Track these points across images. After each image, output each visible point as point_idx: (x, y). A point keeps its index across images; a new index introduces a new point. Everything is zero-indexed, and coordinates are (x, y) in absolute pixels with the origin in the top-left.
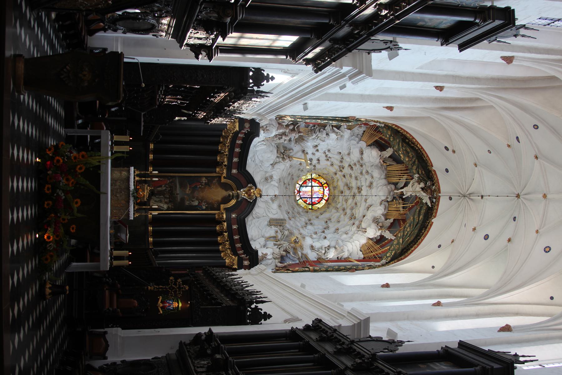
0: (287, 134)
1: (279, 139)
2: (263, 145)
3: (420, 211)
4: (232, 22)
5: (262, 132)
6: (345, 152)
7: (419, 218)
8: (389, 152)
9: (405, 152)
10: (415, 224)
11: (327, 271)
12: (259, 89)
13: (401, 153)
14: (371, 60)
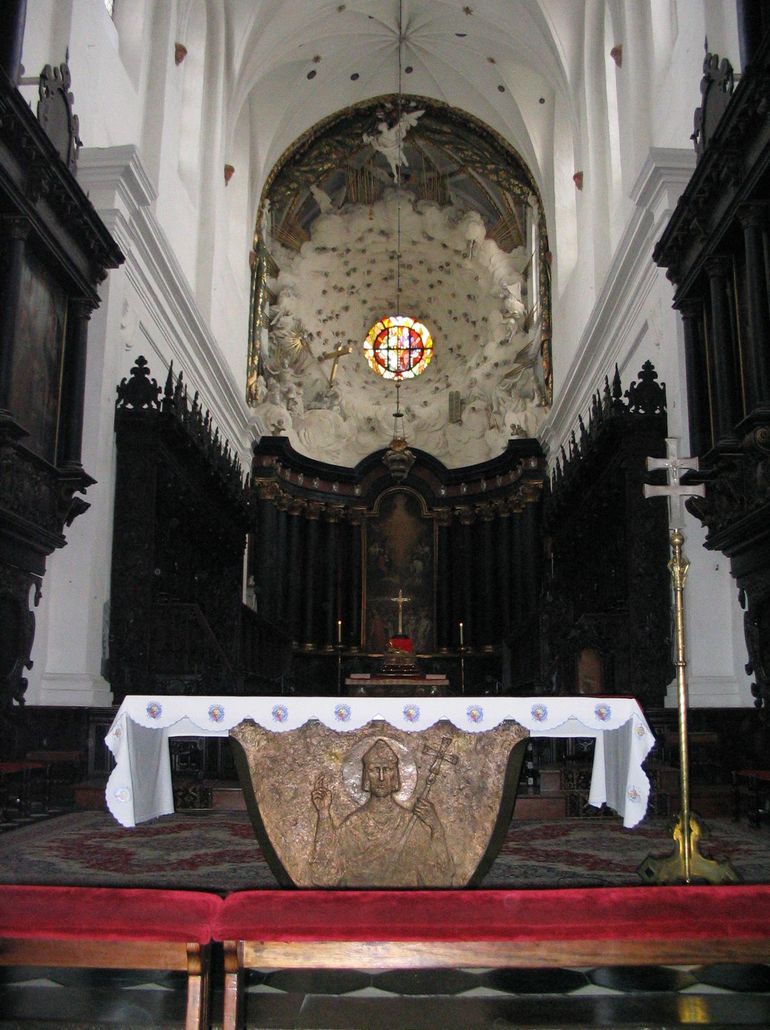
0: (286, 390)
1: (296, 403)
2: (307, 434)
3: (435, 132)
6: (320, 284)
7: (446, 133)
8: (322, 199)
9: (319, 161)
10: (458, 140)
11: (547, 306)
12: (163, 390)
13: (321, 169)
14: (99, 149)
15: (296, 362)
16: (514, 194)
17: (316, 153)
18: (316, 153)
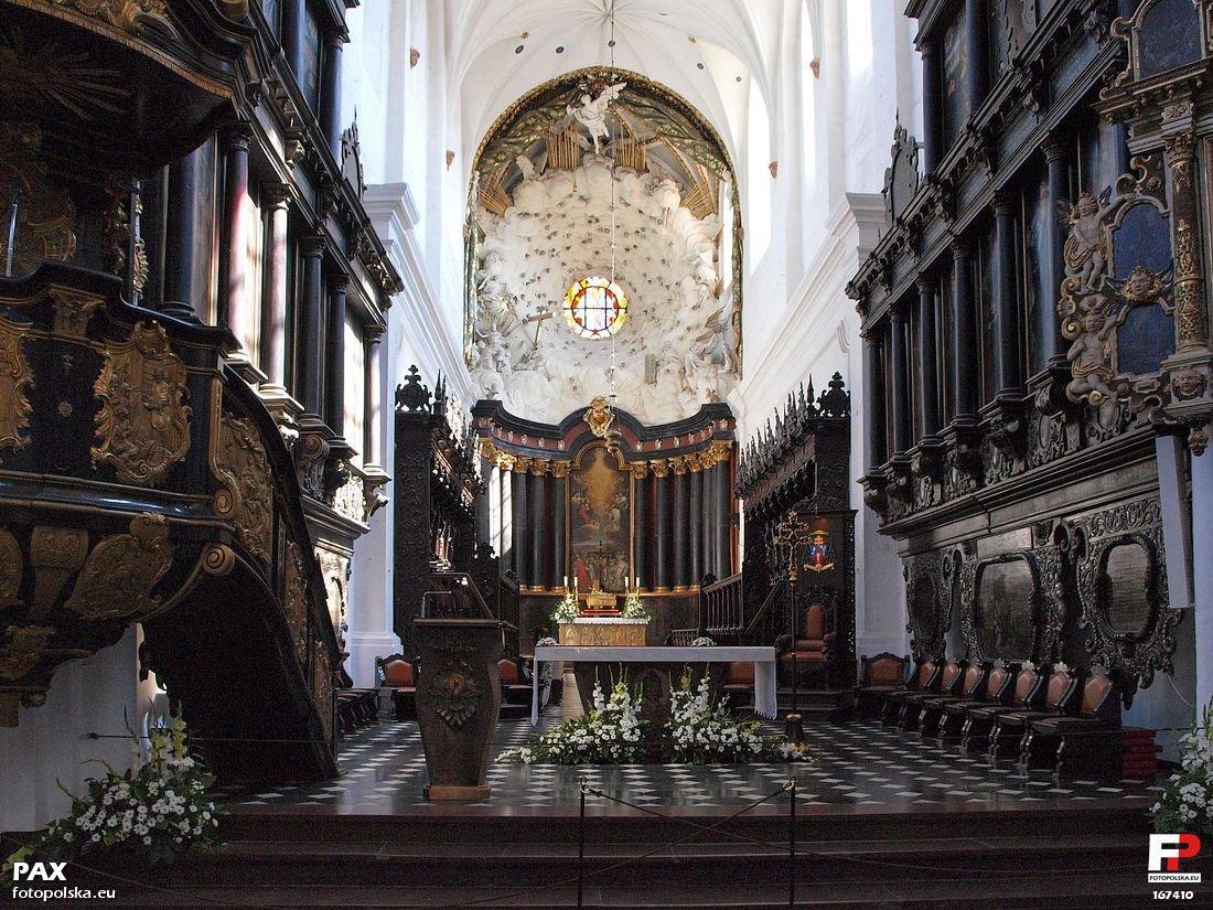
3: (635, 105)
4: (330, 438)
5: (496, 397)
6: (525, 248)
8: (525, 164)
11: (739, 280)
12: (433, 395)
15: (503, 324)
16: (709, 169)
17: (522, 125)
18: (522, 125)
